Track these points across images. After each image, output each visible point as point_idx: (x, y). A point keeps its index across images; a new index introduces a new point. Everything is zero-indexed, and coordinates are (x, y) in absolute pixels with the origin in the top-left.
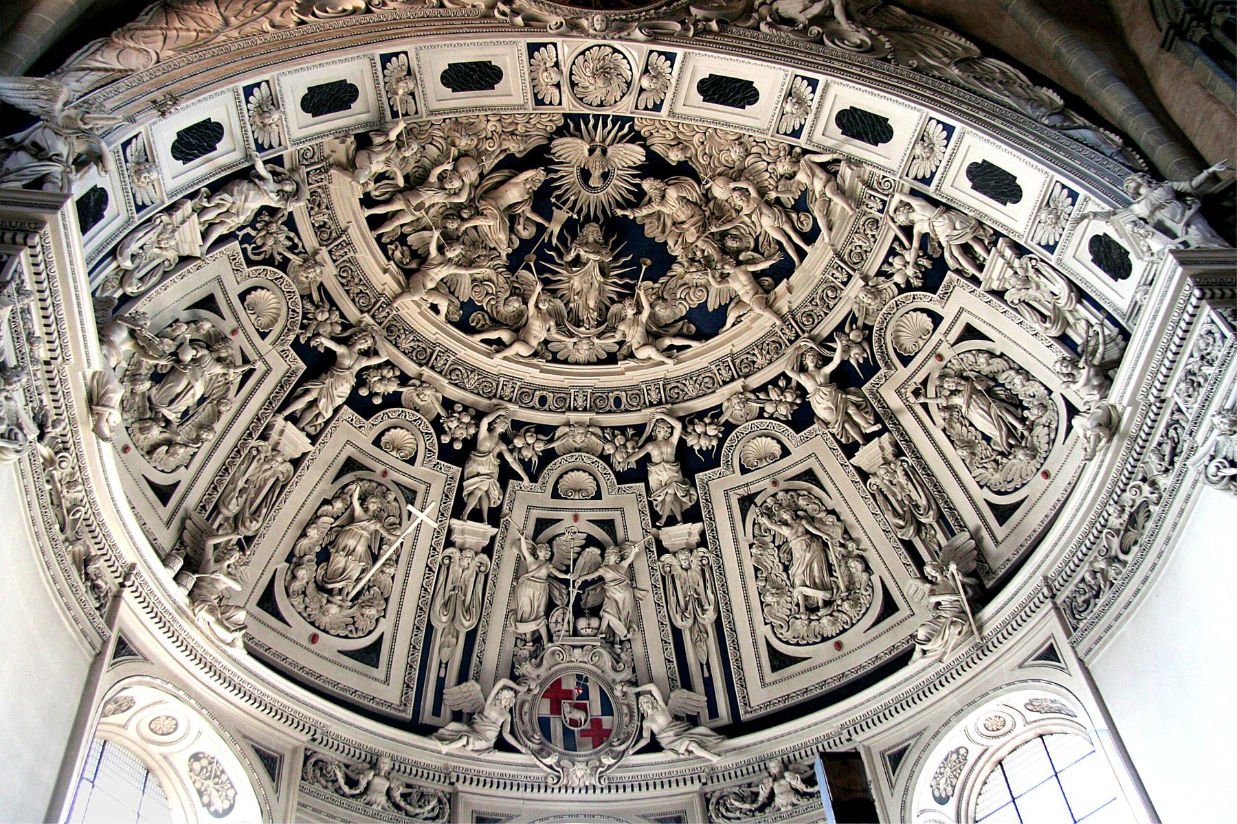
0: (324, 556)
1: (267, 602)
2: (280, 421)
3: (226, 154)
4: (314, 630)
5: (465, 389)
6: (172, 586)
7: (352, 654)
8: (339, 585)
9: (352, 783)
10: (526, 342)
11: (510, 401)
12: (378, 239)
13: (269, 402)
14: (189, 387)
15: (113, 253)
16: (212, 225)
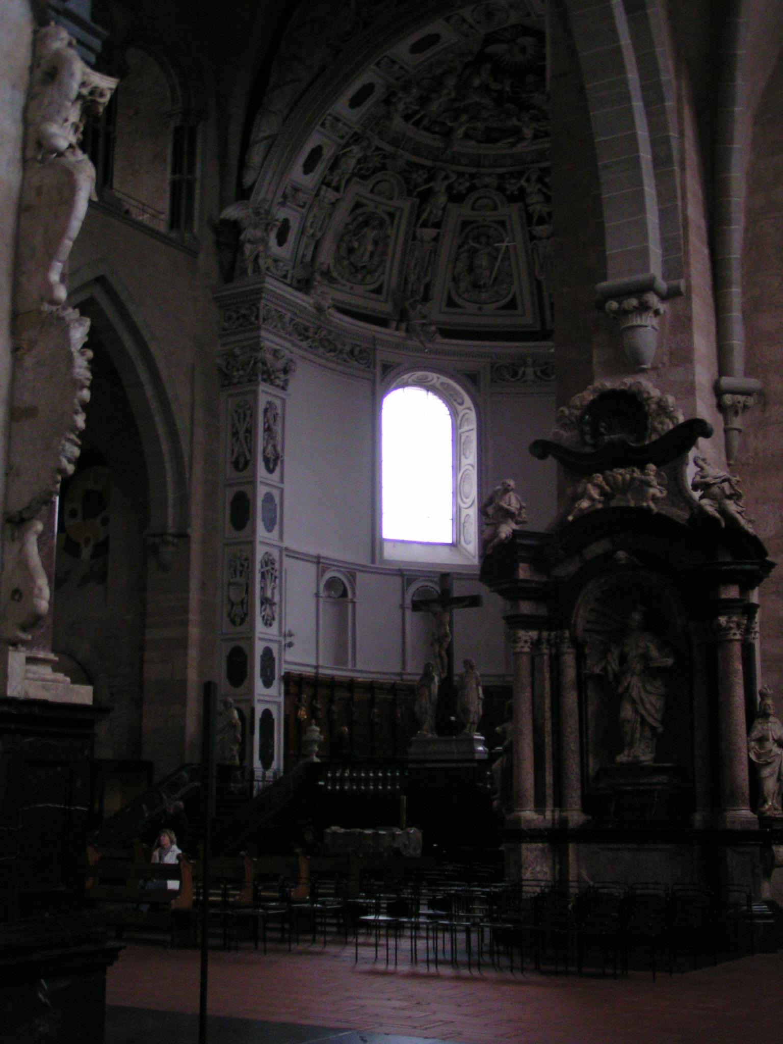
0: (471, 269)
1: (450, 303)
2: (418, 230)
3: (327, 153)
4: (478, 305)
5: (505, 166)
6: (397, 333)
7: (504, 307)
8: (482, 283)
9: (515, 374)
10: (524, 139)
11: (533, 163)
12: (424, 129)
13: (409, 223)
14: (366, 249)
15: (302, 233)
16: (340, 181)
